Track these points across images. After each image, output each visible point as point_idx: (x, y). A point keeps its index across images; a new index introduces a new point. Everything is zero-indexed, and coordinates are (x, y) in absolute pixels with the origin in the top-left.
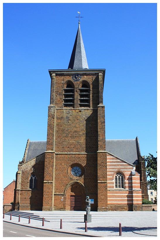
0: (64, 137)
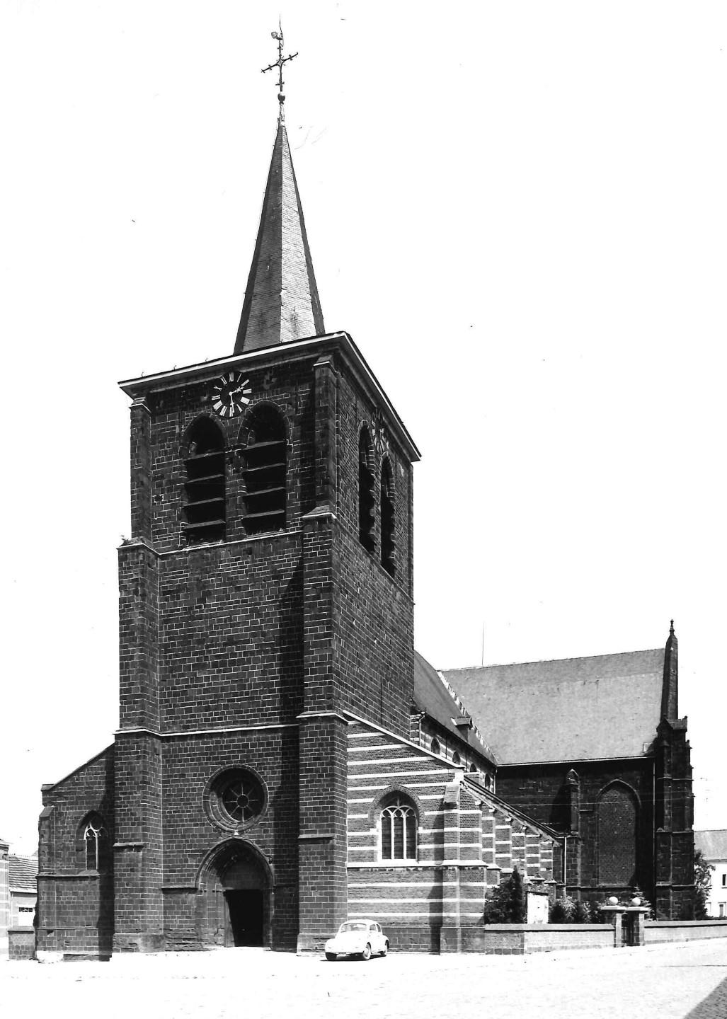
0: (188, 668)
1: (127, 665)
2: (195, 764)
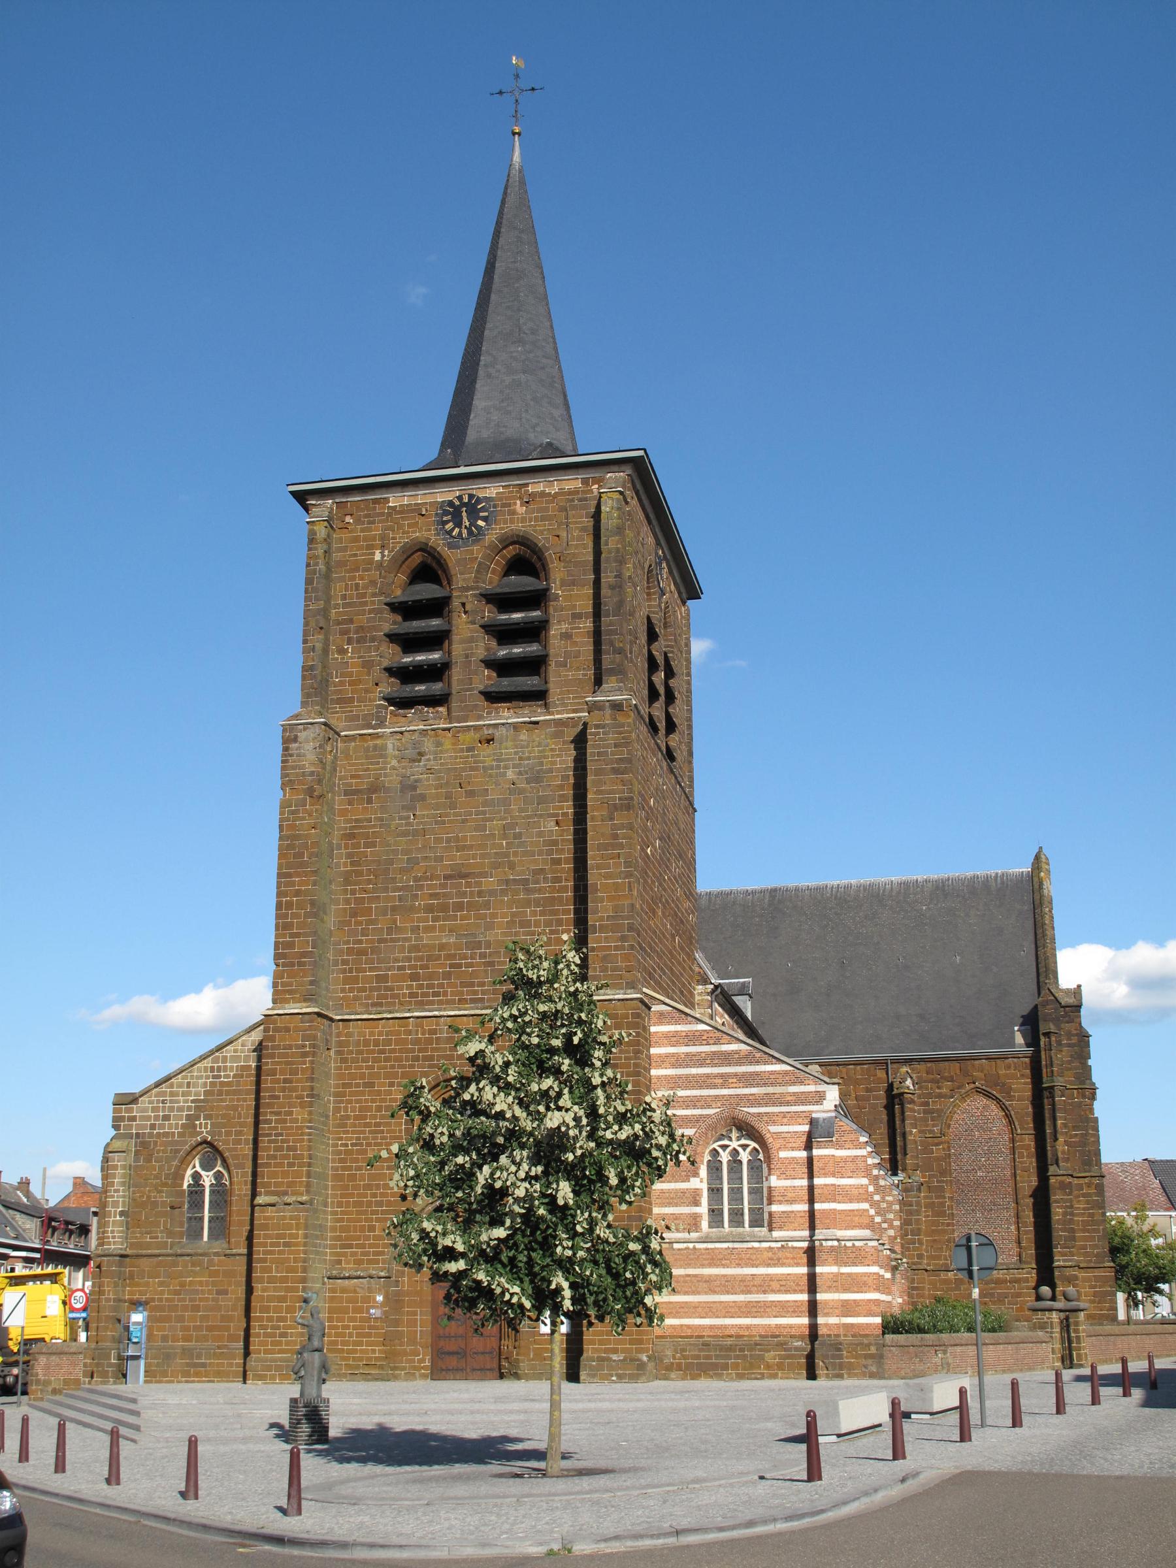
1: (289, 905)
2: (393, 1067)
